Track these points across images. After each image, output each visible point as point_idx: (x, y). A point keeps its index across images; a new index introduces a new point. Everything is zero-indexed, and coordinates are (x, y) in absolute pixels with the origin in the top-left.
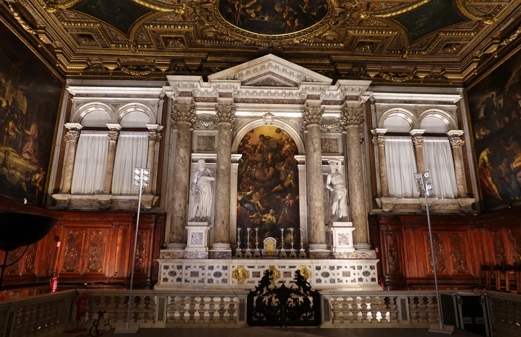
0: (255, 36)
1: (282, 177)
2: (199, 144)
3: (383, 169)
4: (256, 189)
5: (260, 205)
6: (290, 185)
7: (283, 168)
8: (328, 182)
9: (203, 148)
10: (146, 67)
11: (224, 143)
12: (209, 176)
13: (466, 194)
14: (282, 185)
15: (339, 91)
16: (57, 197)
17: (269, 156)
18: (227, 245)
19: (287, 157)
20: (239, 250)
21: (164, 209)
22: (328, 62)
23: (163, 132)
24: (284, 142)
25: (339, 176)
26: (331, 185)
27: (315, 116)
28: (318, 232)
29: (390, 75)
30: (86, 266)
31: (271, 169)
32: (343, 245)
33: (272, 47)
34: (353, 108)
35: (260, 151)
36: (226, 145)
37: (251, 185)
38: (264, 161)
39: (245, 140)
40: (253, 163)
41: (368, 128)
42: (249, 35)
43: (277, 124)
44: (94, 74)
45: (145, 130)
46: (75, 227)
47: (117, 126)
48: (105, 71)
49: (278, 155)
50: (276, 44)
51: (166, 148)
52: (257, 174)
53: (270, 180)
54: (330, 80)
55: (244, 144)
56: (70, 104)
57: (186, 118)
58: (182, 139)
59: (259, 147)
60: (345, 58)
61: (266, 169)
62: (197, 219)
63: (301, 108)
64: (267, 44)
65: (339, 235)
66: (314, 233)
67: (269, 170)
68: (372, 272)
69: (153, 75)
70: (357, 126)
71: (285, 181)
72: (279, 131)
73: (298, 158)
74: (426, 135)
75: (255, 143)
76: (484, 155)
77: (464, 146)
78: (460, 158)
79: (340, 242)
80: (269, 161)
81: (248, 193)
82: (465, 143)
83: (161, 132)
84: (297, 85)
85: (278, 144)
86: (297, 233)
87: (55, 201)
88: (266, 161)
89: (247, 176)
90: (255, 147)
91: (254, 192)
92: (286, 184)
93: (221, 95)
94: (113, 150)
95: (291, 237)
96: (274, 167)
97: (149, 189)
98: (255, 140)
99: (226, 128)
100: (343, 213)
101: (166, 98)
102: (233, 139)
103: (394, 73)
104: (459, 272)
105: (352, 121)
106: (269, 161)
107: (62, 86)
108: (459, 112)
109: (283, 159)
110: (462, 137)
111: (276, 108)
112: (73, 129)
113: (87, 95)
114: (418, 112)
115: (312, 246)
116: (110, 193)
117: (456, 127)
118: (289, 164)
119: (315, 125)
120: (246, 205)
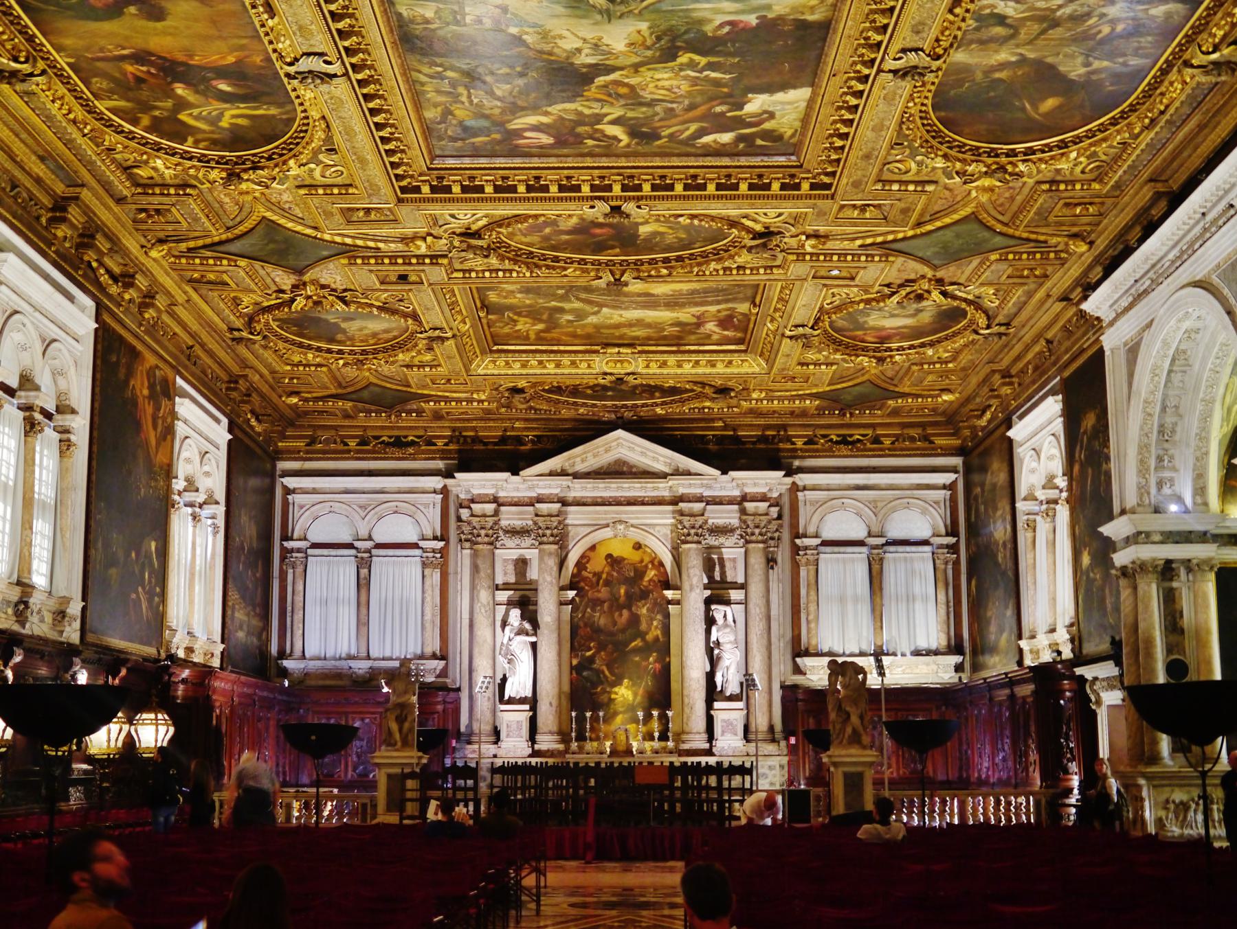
0: (594, 406)
1: (643, 626)
2: (505, 574)
3: (812, 607)
4: (601, 647)
5: (607, 673)
6: (657, 639)
7: (644, 611)
8: (713, 638)
9: (512, 579)
10: (410, 438)
11: (549, 579)
12: (527, 634)
13: (949, 646)
14: (644, 639)
15: (734, 484)
16: (286, 663)
17: (622, 591)
18: (556, 737)
19: (651, 591)
20: (574, 745)
21: (454, 681)
22: (720, 424)
23: (443, 552)
24: (646, 566)
25: (728, 630)
26: (718, 643)
27: (693, 531)
28: (693, 717)
29: (831, 440)
30: (350, 769)
31: (625, 613)
32: (728, 736)
33: (622, 418)
34: (754, 515)
35: (607, 583)
36: (551, 583)
37: (593, 640)
38: (614, 599)
39: (580, 565)
40: (596, 603)
41: (791, 533)
42: (584, 405)
43: (635, 535)
44: (324, 452)
45: (415, 546)
46: (328, 713)
47: (369, 544)
48: (342, 447)
49: (637, 589)
50: (628, 414)
51: (451, 578)
52: (602, 622)
53: (623, 631)
54: (718, 473)
55: (579, 571)
56: (286, 504)
57: (486, 539)
58: (482, 574)
59: (604, 576)
60: (748, 421)
61: (617, 614)
62: (511, 701)
63: (674, 512)
64: (613, 416)
65: (723, 721)
66: (688, 718)
67: (621, 615)
68: (770, 773)
69: (424, 452)
70: (761, 545)
71: (647, 633)
72: (638, 546)
73: (669, 594)
74: (888, 544)
75: (598, 569)
76: (973, 583)
77: (956, 563)
78: (947, 585)
79: (723, 733)
80: (622, 599)
81: (588, 654)
82: (958, 558)
83: (441, 551)
84: (664, 476)
85: (636, 570)
86: (664, 719)
87: (284, 673)
88: (617, 600)
89: (586, 625)
90: (598, 575)
91: (598, 652)
92: (649, 637)
93: (540, 500)
94: (363, 585)
95: (655, 726)
96: (630, 609)
97: (428, 651)
98: (598, 564)
99: (550, 554)
100: (733, 688)
101: (445, 491)
102: (562, 564)
103: (838, 436)
104: (911, 773)
105: (754, 538)
106: (622, 599)
107: (272, 475)
108: (953, 500)
109: (644, 595)
110: (953, 548)
111: (632, 513)
112: (299, 550)
113: (315, 491)
114: (879, 504)
115: (684, 737)
116: (368, 657)
117: (943, 531)
118: (655, 604)
119: (694, 546)
120: (585, 674)
